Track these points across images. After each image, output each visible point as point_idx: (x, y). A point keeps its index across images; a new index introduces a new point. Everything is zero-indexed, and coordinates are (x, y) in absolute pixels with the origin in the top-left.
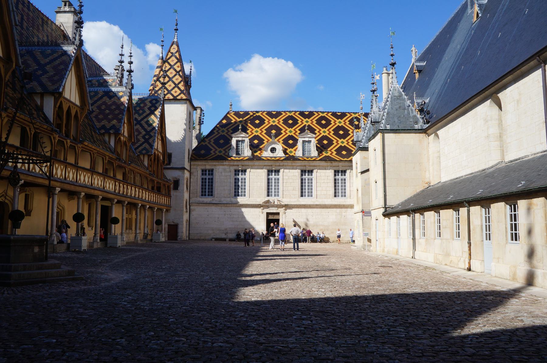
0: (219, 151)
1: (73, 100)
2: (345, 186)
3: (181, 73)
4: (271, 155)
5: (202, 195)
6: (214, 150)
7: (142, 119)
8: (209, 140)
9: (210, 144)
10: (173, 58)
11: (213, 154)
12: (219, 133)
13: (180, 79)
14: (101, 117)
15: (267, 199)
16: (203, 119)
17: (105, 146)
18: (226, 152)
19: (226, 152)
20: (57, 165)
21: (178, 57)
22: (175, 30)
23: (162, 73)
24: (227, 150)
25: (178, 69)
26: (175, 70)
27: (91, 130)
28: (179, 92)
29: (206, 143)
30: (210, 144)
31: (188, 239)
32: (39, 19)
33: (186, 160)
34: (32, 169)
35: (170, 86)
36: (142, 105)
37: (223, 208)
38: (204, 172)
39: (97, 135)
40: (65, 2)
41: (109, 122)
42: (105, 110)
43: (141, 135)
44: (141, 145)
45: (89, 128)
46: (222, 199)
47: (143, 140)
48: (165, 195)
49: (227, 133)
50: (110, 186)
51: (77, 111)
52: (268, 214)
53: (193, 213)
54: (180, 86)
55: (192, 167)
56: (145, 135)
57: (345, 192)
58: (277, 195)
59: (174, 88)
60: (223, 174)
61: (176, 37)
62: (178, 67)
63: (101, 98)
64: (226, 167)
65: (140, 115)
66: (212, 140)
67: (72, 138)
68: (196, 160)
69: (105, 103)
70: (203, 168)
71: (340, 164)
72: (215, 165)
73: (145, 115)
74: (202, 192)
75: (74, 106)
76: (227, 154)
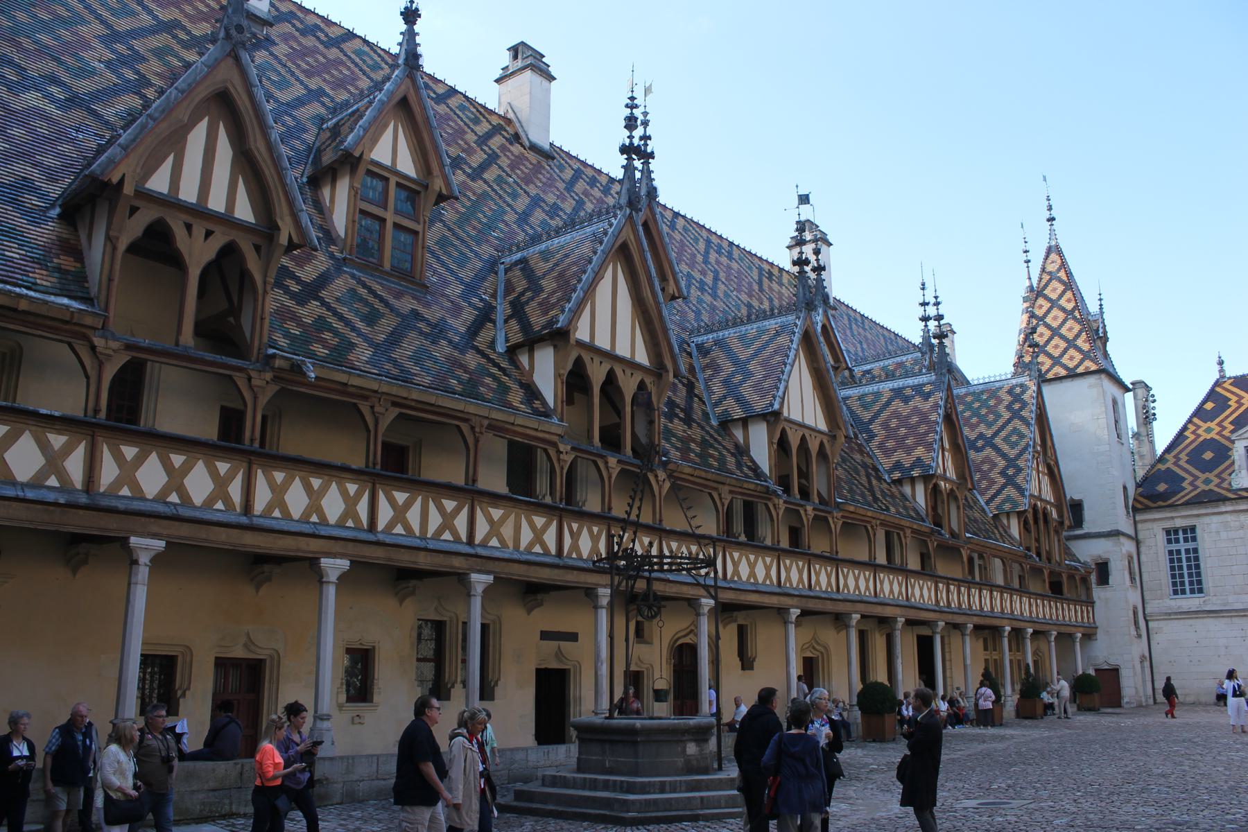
0: (1205, 482)
1: (809, 421)
3: (1077, 314)
5: (1175, 592)
6: (1190, 479)
7: (996, 434)
8: (1176, 457)
9: (1179, 466)
10: (1055, 284)
11: (1190, 488)
13: (1077, 328)
14: (890, 444)
16: (1154, 408)
17: (905, 508)
18: (1223, 480)
19: (1223, 480)
20: (788, 562)
21: (1065, 278)
22: (1048, 220)
23: (1035, 322)
24: (1224, 475)
25: (1070, 306)
26: (1063, 309)
27: (868, 476)
28: (1078, 357)
29: (1169, 465)
30: (1179, 466)
31: (1151, 701)
32: (750, 268)
33: (1122, 511)
34: (733, 576)
35: (1056, 346)
36: (992, 403)
37: (1236, 620)
38: (1171, 534)
39: (885, 486)
41: (909, 454)
42: (898, 427)
43: (997, 470)
44: (999, 492)
45: (863, 473)
48: (1076, 602)
49: (1219, 433)
50: (922, 593)
51: (822, 444)
53: (1155, 639)
54: (1079, 342)
55: (1140, 526)
56: (1007, 468)
60: (1224, 535)
62: (1069, 301)
63: (888, 403)
64: (1228, 517)
65: (989, 425)
66: (1183, 456)
67: (817, 501)
68: (1147, 509)
69: (895, 414)
70: (1168, 525)
72: (1198, 516)
73: (1000, 423)
74: (1174, 584)
75: (814, 434)
76: (1225, 485)
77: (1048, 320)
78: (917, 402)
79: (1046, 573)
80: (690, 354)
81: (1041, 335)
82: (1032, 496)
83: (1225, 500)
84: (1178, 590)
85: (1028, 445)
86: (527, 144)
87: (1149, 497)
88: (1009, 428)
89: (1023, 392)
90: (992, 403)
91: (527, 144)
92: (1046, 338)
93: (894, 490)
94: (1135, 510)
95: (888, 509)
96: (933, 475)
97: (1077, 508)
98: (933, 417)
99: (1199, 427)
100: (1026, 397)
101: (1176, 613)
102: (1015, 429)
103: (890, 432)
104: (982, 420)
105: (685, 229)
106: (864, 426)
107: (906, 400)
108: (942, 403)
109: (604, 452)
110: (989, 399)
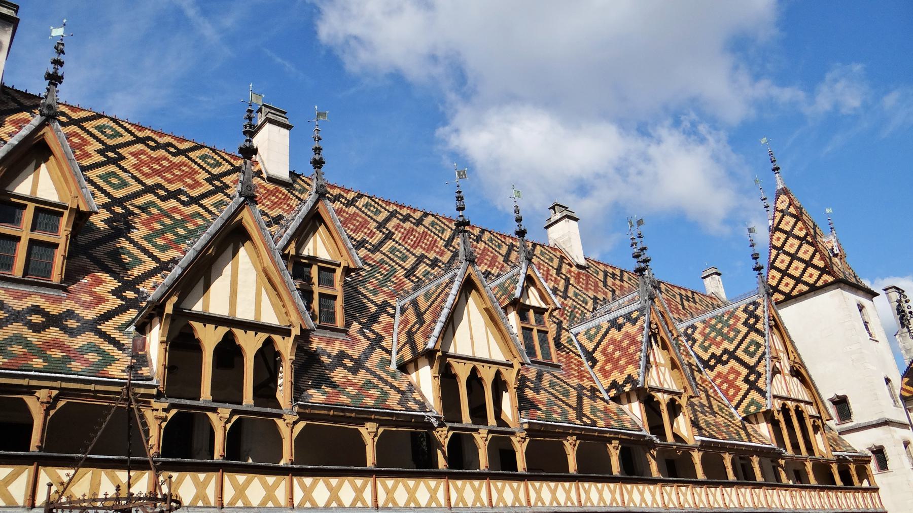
10: (787, 218)
13: (812, 249)
14: (608, 367)
21: (795, 213)
22: (774, 170)
23: (774, 252)
26: (797, 237)
35: (797, 268)
36: (731, 322)
39: (600, 405)
40: (553, 208)
41: (622, 373)
42: (614, 351)
44: (745, 396)
47: (746, 386)
51: (498, 373)
54: (817, 261)
56: (748, 375)
59: (805, 270)
61: (779, 181)
62: (801, 229)
65: (731, 341)
69: (613, 341)
73: (740, 337)
77: (786, 248)
78: (628, 328)
79: (809, 466)
80: (393, 316)
81: (782, 261)
82: (775, 397)
85: (764, 353)
86: (265, 176)
88: (748, 340)
89: (756, 309)
90: (731, 322)
91: (265, 176)
92: (786, 263)
93: (613, 406)
94: (903, 398)
95: (594, 423)
96: (642, 388)
97: (841, 403)
98: (639, 338)
100: (759, 312)
102: (752, 340)
103: (609, 358)
104: (726, 337)
105: (433, 224)
106: (590, 356)
107: (619, 328)
108: (645, 325)
109: (215, 405)
110: (729, 318)
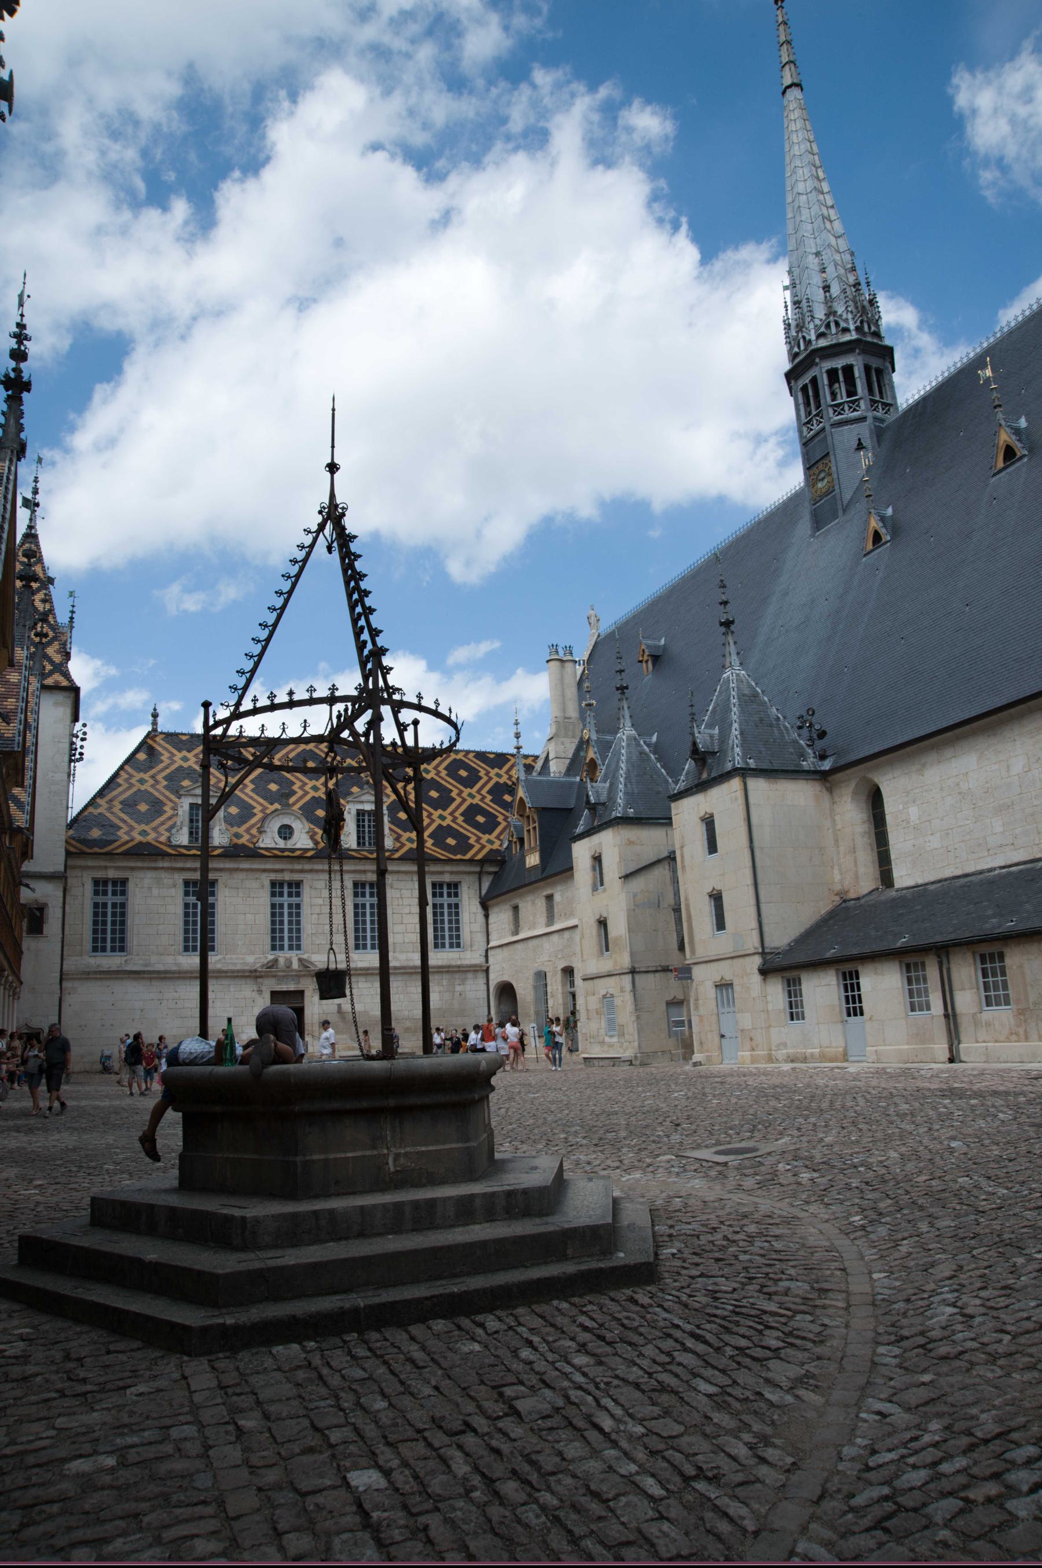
2: (457, 921)
4: (281, 844)
5: (95, 949)
6: (125, 828)
12: (132, 785)
15: (271, 957)
16: (82, 747)
37: (155, 983)
38: (100, 885)
46: (154, 959)
52: (274, 994)
57: (458, 937)
58: (296, 945)
60: (155, 892)
64: (163, 874)
66: (117, 807)
68: (81, 854)
70: (100, 874)
71: (448, 868)
72: (133, 869)
74: (95, 940)
83: (164, 855)
84: (98, 946)
87: (80, 841)
94: (69, 854)
99: (131, 776)
101: (95, 972)
